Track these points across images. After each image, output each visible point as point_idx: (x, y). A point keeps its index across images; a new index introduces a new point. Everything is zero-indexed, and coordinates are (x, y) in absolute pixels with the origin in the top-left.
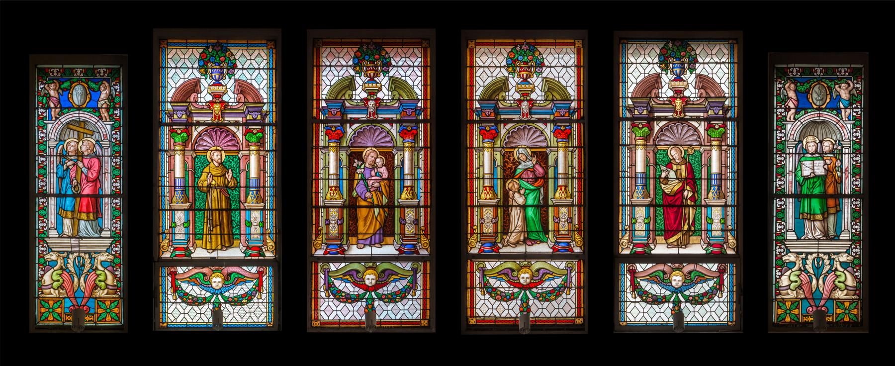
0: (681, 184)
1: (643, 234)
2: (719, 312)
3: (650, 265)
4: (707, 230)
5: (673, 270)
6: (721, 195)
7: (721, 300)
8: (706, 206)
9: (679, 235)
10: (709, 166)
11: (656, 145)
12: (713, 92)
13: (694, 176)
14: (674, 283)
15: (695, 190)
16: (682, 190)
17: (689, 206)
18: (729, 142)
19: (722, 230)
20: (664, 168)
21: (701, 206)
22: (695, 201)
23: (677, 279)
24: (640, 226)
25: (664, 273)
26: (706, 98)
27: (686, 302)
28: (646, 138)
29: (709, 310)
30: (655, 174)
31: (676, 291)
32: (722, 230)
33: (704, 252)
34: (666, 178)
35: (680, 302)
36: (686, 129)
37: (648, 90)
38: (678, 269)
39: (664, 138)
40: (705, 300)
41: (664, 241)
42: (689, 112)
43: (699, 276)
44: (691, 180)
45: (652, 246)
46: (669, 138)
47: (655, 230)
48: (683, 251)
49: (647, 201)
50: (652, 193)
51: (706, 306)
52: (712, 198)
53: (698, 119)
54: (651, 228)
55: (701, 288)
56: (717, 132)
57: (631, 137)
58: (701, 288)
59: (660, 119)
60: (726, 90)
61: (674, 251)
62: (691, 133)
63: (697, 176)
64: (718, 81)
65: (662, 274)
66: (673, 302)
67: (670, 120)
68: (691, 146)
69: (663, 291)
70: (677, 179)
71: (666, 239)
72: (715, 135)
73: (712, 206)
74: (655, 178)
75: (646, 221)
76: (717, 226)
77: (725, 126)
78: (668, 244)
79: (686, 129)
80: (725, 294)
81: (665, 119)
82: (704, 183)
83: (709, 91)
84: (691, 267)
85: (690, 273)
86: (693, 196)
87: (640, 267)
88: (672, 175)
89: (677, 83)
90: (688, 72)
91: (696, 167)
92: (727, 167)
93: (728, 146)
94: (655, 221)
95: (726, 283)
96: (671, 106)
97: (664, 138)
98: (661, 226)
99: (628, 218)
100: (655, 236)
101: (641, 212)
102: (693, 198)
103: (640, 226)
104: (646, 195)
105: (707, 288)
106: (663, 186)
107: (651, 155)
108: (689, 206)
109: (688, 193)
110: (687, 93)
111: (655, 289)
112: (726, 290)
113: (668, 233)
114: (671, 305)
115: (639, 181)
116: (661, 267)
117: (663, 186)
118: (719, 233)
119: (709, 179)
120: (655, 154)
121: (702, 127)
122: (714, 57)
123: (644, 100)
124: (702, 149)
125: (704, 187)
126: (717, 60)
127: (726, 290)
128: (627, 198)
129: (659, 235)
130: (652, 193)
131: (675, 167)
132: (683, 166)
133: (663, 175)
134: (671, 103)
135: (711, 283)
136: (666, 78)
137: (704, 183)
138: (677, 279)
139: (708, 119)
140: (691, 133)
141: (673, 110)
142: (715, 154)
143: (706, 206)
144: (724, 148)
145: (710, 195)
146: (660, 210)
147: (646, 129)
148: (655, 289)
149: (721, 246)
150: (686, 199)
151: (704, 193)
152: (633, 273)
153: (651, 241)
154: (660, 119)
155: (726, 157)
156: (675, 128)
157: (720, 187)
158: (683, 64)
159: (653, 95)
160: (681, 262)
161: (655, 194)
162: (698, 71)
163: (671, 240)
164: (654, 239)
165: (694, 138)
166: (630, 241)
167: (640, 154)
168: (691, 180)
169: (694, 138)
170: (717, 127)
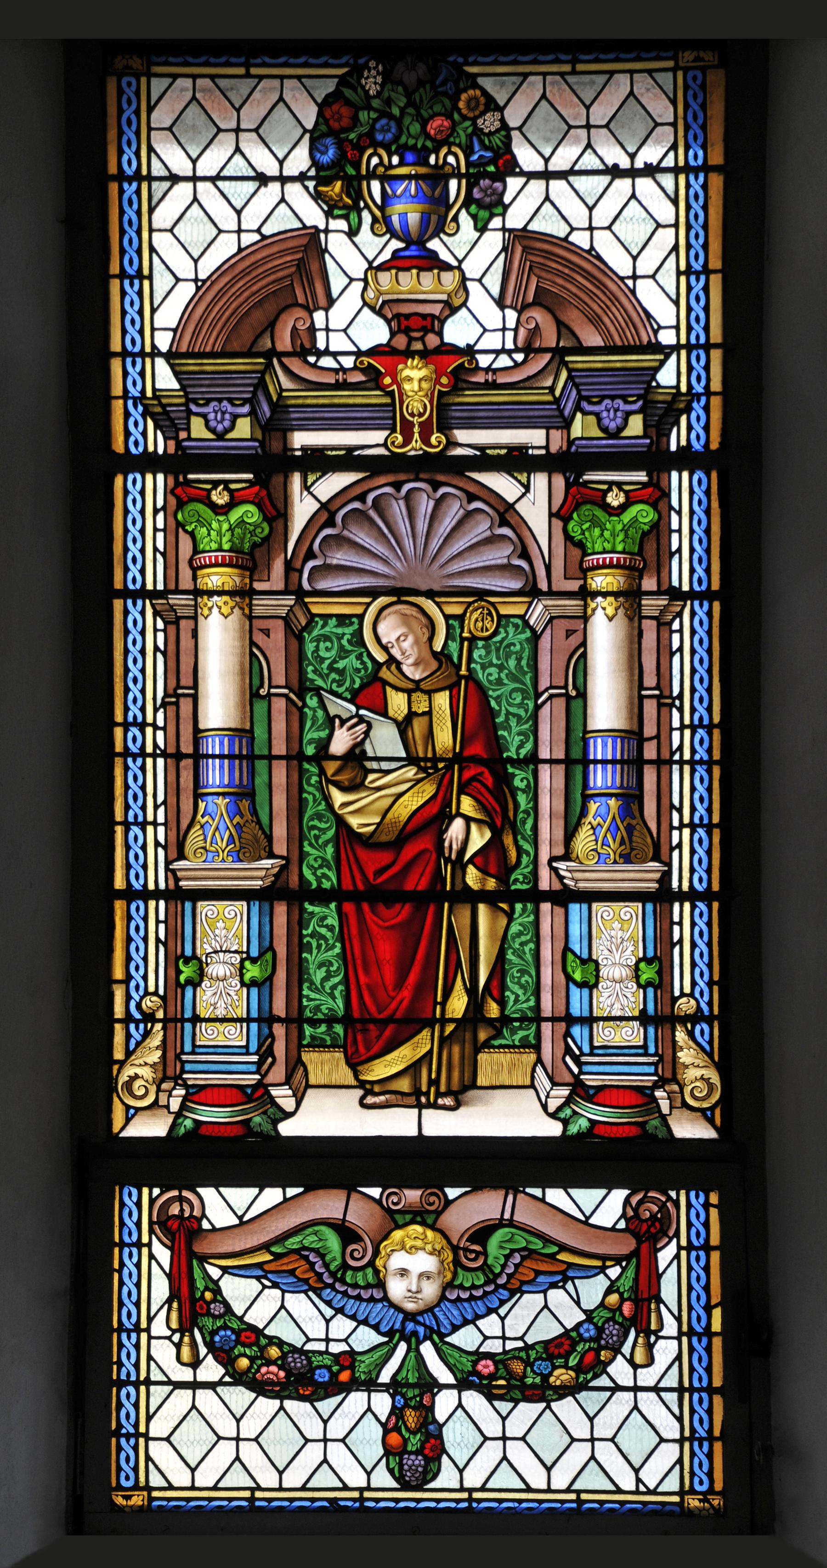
0: (428, 790)
1: (234, 1035)
2: (637, 1440)
3: (272, 1196)
4: (570, 1020)
5: (395, 1219)
6: (639, 839)
7: (647, 1377)
8: (564, 897)
9: (422, 1043)
10: (577, 698)
11: (300, 594)
12: (596, 321)
13: (497, 745)
14: (397, 1289)
15: (501, 817)
16: (437, 815)
17: (473, 898)
18: (680, 574)
19: (643, 1018)
20: (342, 707)
21: (535, 896)
22: (504, 872)
23: (412, 1268)
24: (221, 995)
25: (347, 1234)
26: (559, 353)
27: (462, 1385)
28: (249, 559)
29: (581, 1430)
30: (295, 736)
31: (410, 1327)
32: (643, 1018)
33: (554, 1129)
34: (356, 757)
35: (431, 1386)
36: (453, 512)
37: (259, 317)
38: (418, 1215)
39: (339, 557)
40: (561, 1376)
41: (345, 1075)
42: (471, 424)
43: (529, 1253)
44: (483, 767)
45: (283, 1096)
46: (367, 556)
47: (296, 1019)
48: (440, 1124)
49: (260, 871)
50: (280, 830)
51: (566, 1407)
52: (592, 856)
53: (516, 461)
54: (279, 1008)
55: (535, 1317)
56: (615, 524)
57: (170, 555)
58: (535, 1317)
59: (319, 461)
60: (663, 312)
61: (398, 1123)
62: (481, 528)
63: (514, 744)
64: (621, 264)
65: (333, 1242)
66: (395, 1387)
67: (372, 466)
68: (481, 594)
69: (342, 1326)
70: (411, 760)
71: (354, 1065)
72: (607, 539)
73: (589, 897)
74: (295, 757)
75: (253, 971)
76: (618, 994)
77: (657, 496)
78: (367, 1088)
79: (453, 512)
80: (665, 1351)
81: (348, 460)
82: (550, 779)
83: (574, 319)
84: (486, 1206)
85: (481, 1234)
86: (494, 846)
87: (221, 1206)
88: (385, 740)
89: (407, 279)
90: (465, 219)
91: (507, 701)
92: (666, 701)
93: (675, 594)
94: (298, 974)
95: (668, 1290)
96: (375, 397)
97: (339, 557)
98: (326, 996)
99: (156, 957)
100: (297, 1048)
101: (223, 928)
102: (492, 858)
103: (221, 995)
104: (252, 841)
105: (572, 1317)
106: (338, 797)
107: (275, 644)
108: (473, 898)
109: (467, 835)
110: (458, 331)
111: (300, 1320)
112: (670, 1327)
113: (363, 1035)
114: (382, 1403)
115: (215, 775)
116: (329, 1205)
117: (338, 797)
118: (630, 1034)
119: (576, 761)
120: (295, 635)
121: (535, 502)
122: (601, 139)
123: (239, 364)
124: (537, 613)
125: (550, 802)
126: (615, 156)
127: (670, 1327)
128: (156, 858)
129: (317, 1044)
130: (280, 830)
131: (398, 703)
132: (442, 700)
133: (341, 742)
134: (374, 379)
135: (593, 1291)
136: (350, 255)
137: (550, 779)
138: (412, 1268)
139: (567, 463)
140: (481, 528)
141: (388, 415)
142: (605, 635)
143: (564, 897)
144: (651, 605)
145: (583, 841)
146: (325, 918)
147: (249, 513)
148: (300, 1320)
149: (644, 1098)
150: (460, 865)
151: (549, 831)
152: (186, 1235)
153: (278, 1073)
154: (319, 461)
155: (665, 652)
156: (398, 509)
157: (631, 798)
158: (438, 178)
159: (284, 343)
160: (434, 1183)
161: (298, 835)
162: (516, 219)
163: (380, 1070)
164: (295, 1065)
165: (499, 555)
166: (170, 1072)
167: (218, 638)
168: (483, 767)
169: (499, 555)
170: (615, 499)
